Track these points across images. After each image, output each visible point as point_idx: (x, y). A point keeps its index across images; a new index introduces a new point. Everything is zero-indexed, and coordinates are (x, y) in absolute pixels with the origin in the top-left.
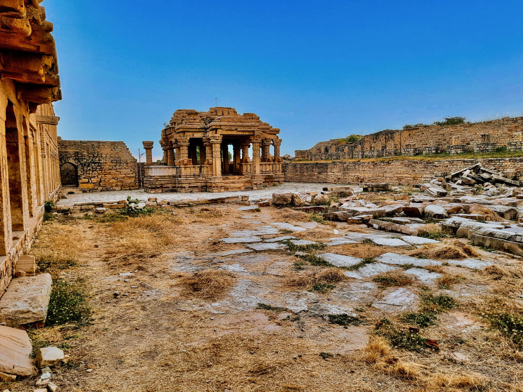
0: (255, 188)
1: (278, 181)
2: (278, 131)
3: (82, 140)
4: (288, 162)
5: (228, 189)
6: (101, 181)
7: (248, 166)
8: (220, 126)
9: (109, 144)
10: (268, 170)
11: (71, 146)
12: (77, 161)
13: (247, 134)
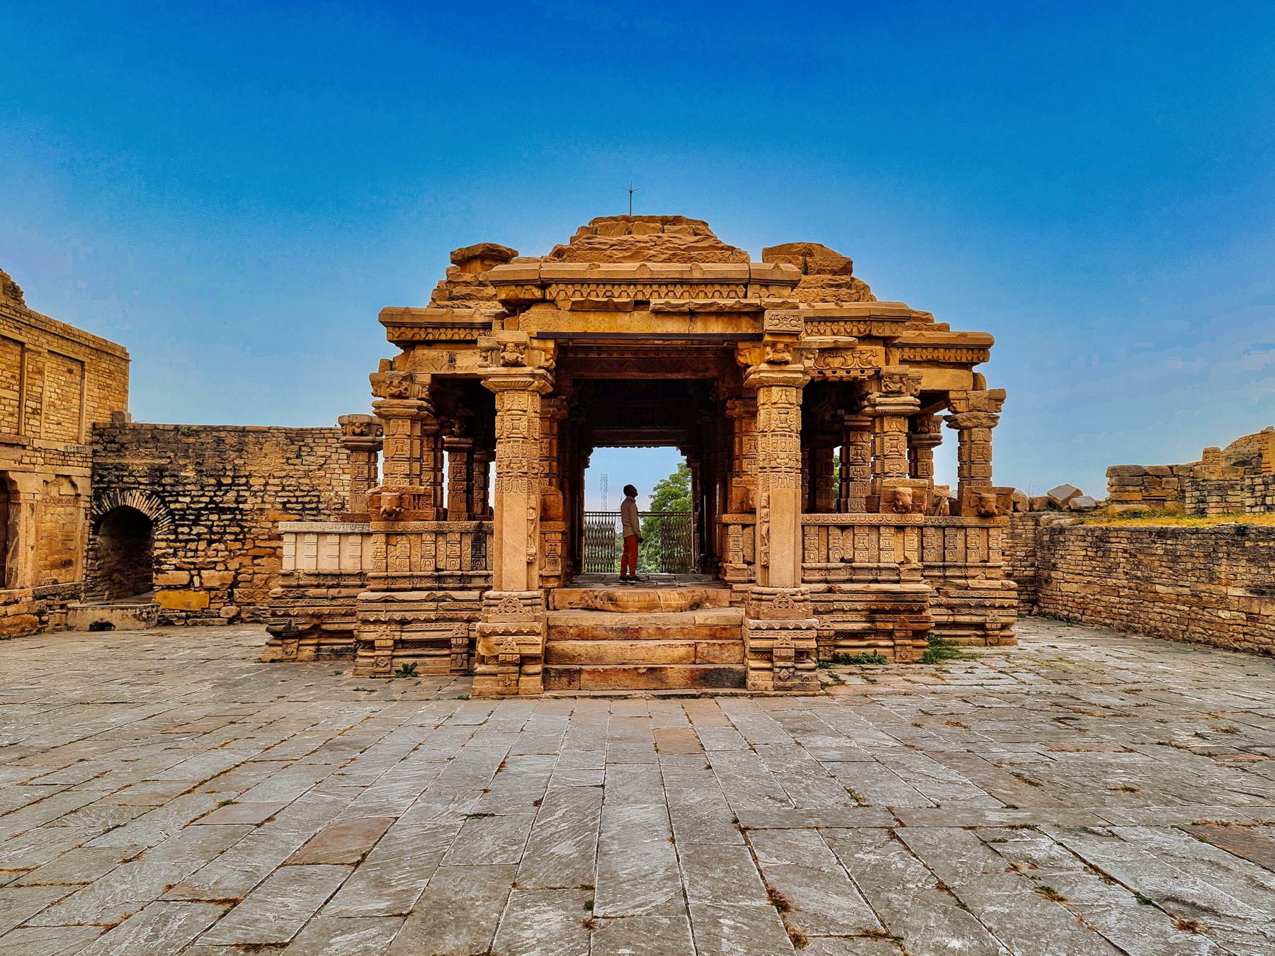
0: (760, 680)
1: (980, 626)
2: (980, 349)
3: (184, 421)
4: (1066, 521)
5: (572, 675)
6: (235, 584)
8: (544, 285)
9: (282, 439)
10: (890, 559)
12: (156, 501)
13: (716, 327)
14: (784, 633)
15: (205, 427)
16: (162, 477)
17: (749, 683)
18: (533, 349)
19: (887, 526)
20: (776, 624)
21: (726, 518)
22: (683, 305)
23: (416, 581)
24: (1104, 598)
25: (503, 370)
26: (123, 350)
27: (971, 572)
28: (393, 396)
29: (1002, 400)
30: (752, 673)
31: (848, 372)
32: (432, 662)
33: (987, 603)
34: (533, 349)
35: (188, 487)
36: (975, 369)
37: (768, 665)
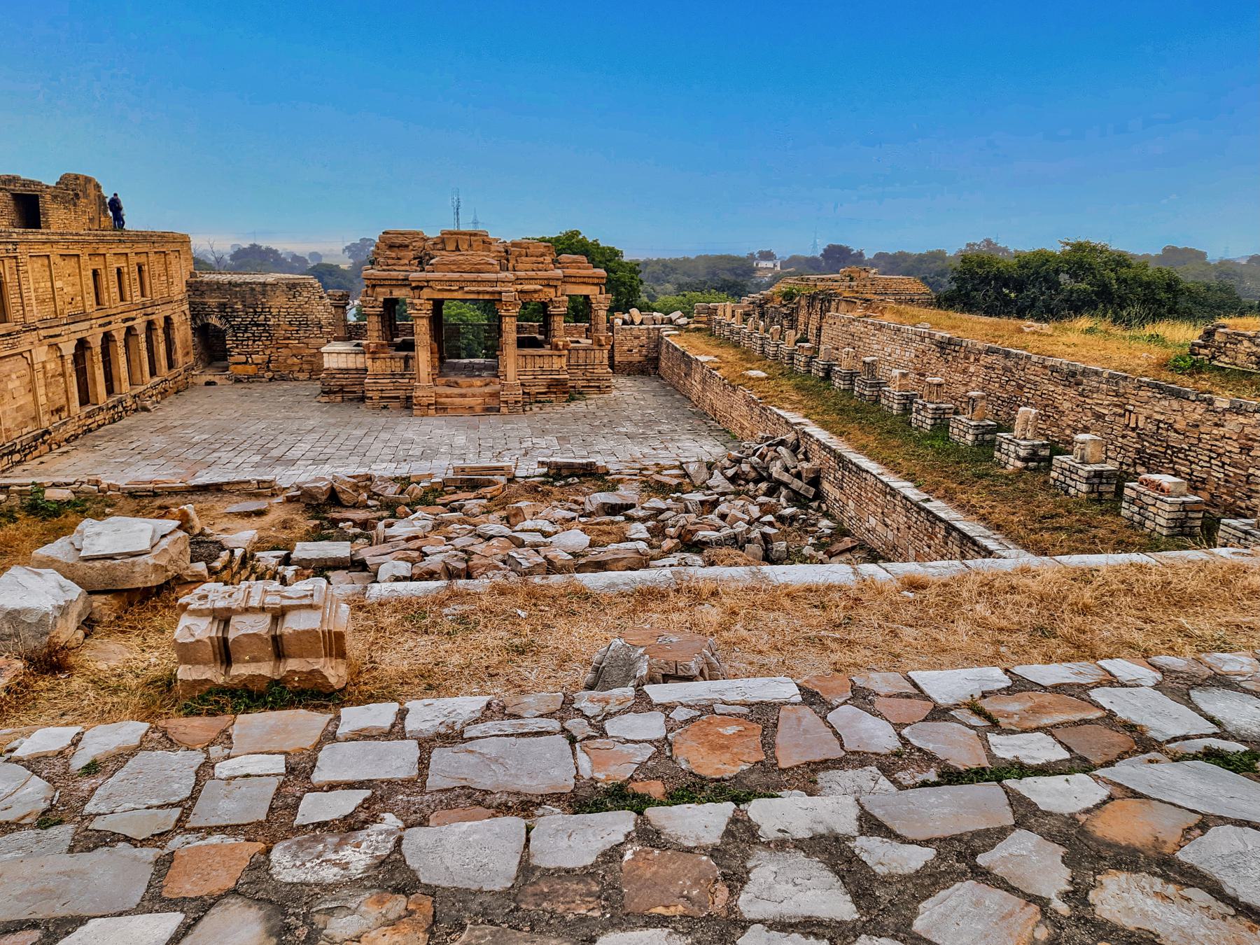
0: (504, 410)
5: (445, 409)
6: (270, 361)
10: (555, 367)
11: (213, 290)
12: (224, 321)
32: (395, 404)
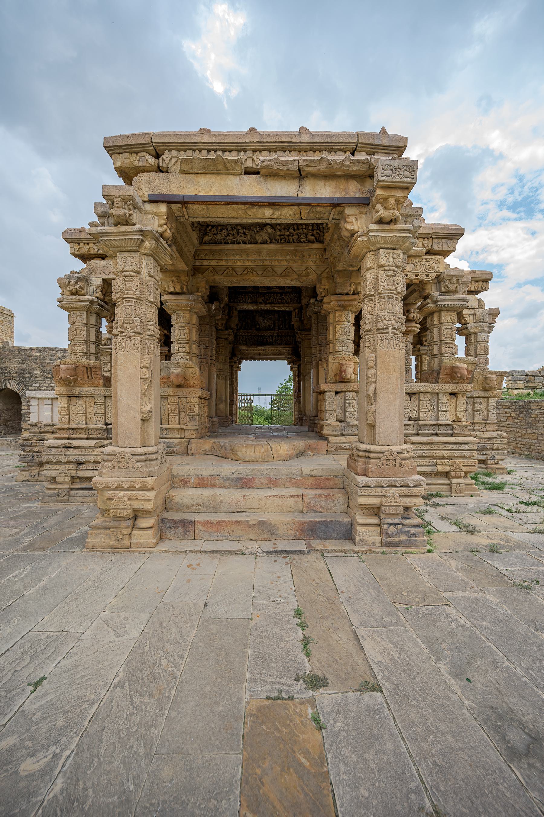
0: (367, 534)
7: (351, 397)
10: (446, 418)
12: (22, 385)
13: (324, 191)
14: (392, 490)
15: (45, 348)
16: (24, 374)
17: (358, 538)
18: (146, 213)
19: (445, 393)
20: (384, 481)
21: (323, 386)
22: (292, 162)
23: (90, 432)
24: (524, 440)
25: (113, 229)
26: (10, 311)
27: (477, 427)
28: (72, 293)
29: (496, 315)
30: (359, 528)
31: (417, 276)
33: (489, 447)
34: (146, 213)
35: (38, 379)
36: (479, 296)
37: (376, 521)
